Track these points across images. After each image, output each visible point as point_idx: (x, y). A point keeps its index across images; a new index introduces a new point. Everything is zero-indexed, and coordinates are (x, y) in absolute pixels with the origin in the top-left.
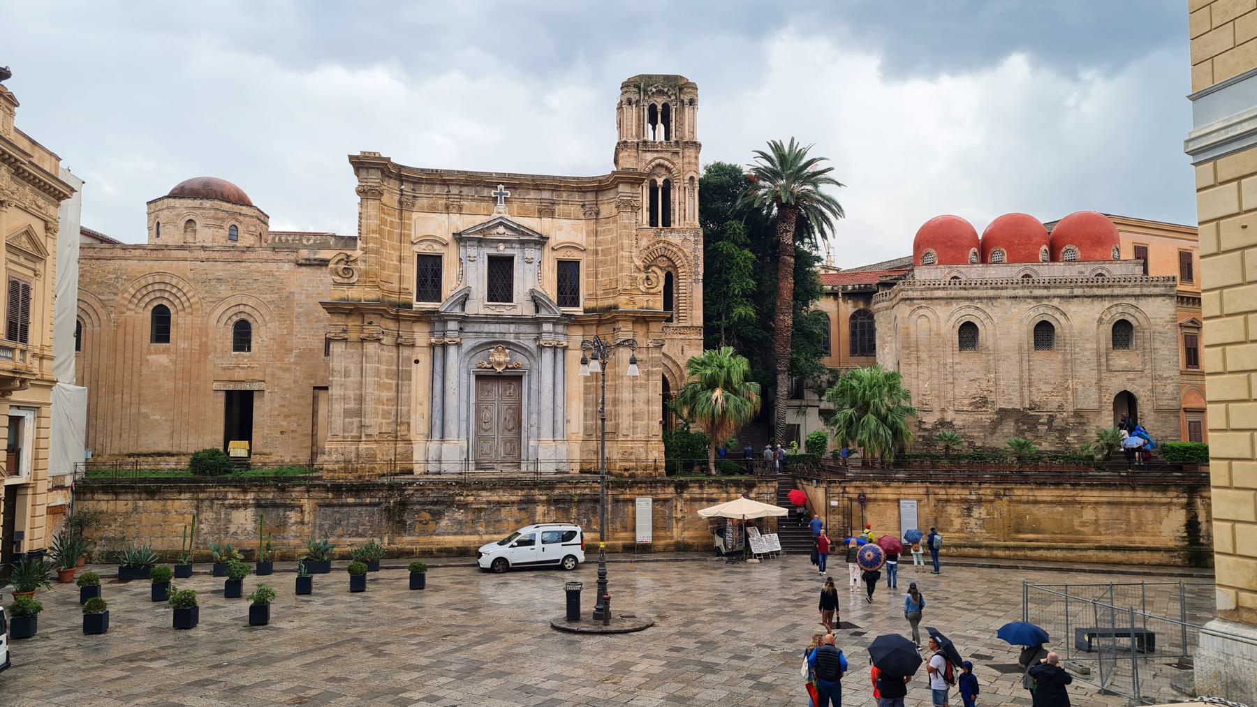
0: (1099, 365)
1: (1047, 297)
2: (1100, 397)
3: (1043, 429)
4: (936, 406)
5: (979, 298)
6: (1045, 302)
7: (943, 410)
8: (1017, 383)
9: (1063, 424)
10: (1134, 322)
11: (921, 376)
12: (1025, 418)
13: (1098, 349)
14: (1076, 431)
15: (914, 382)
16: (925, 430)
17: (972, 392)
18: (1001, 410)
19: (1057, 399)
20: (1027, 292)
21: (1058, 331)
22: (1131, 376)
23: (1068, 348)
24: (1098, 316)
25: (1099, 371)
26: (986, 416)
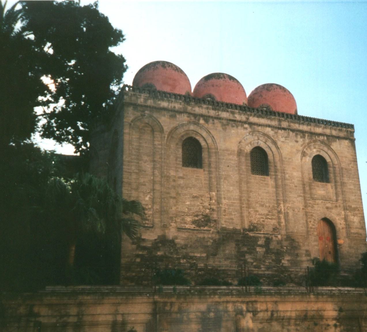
0: (304, 192)
1: (260, 125)
6: (260, 128)
9: (278, 247)
10: (328, 160)
12: (243, 239)
13: (303, 178)
14: (290, 254)
16: (145, 248)
17: (194, 209)
18: (224, 229)
19: (274, 222)
20: (243, 118)
21: (270, 157)
23: (279, 175)
24: (301, 148)
26: (209, 234)
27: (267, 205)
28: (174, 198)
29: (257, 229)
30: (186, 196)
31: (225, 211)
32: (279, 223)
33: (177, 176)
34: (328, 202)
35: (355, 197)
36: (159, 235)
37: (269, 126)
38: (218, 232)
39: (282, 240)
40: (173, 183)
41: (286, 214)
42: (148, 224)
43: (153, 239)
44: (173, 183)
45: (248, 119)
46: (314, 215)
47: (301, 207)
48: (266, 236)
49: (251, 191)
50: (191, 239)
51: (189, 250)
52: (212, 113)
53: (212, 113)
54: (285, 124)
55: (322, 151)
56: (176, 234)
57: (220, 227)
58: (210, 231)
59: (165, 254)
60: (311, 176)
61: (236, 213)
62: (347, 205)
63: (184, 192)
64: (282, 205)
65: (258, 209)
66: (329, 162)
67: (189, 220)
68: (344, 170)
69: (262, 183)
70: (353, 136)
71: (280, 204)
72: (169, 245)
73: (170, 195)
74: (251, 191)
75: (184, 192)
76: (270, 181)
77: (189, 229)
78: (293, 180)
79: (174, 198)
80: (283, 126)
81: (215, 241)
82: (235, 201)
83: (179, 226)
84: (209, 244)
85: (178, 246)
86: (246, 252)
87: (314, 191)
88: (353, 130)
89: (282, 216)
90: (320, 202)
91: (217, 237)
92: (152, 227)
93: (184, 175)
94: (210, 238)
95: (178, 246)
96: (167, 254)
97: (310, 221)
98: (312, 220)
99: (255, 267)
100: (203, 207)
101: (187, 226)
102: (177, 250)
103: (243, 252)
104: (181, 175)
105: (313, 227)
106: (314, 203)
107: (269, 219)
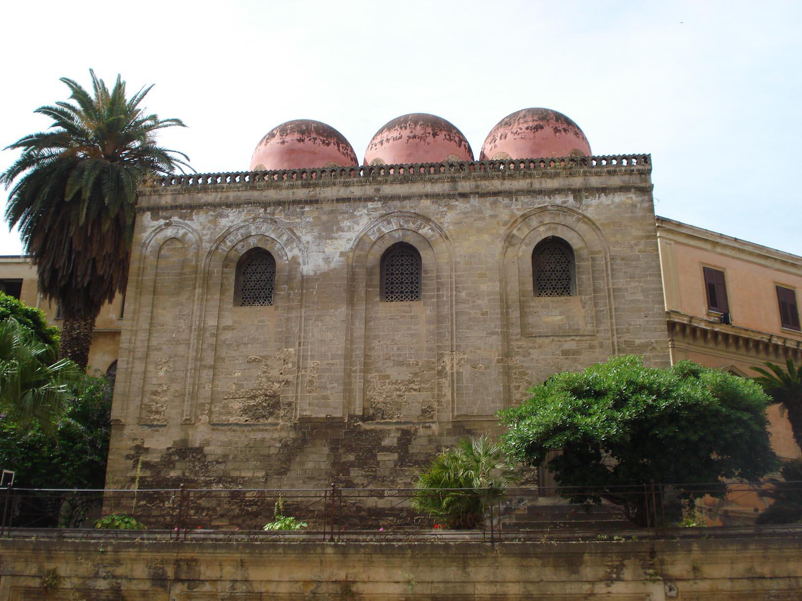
2: (508, 390)
3: (387, 459)
4: (174, 414)
5: (279, 203)
7: (188, 423)
8: (339, 365)
9: (431, 449)
11: (155, 356)
12: (349, 438)
15: (139, 367)
16: (146, 465)
17: (251, 384)
18: (304, 420)
20: (369, 190)
22: (570, 345)
23: (444, 292)
24: (503, 231)
25: (506, 337)
26: (276, 433)
27: (412, 361)
28: (210, 367)
29: (383, 414)
30: (236, 362)
31: (311, 382)
32: (439, 398)
33: (221, 327)
34: (568, 339)
35: (646, 319)
36: (177, 439)
37: (427, 196)
38: (295, 427)
39: (441, 434)
40: (212, 341)
41: (455, 375)
42: (158, 420)
43: (164, 447)
44: (212, 341)
45: (378, 190)
46: (529, 371)
47: (495, 357)
48: (404, 427)
49: (376, 337)
50: (236, 443)
51: (230, 466)
52: (302, 193)
53: (302, 193)
54: (465, 186)
55: (560, 227)
56: (207, 437)
57: (298, 417)
58: (277, 424)
59: (184, 473)
60: (530, 287)
61: (335, 385)
62: (622, 340)
63: (234, 354)
64: (446, 359)
65: (389, 372)
66: (580, 249)
67: (236, 407)
68: (618, 261)
69: (402, 317)
70: (648, 180)
71: (440, 356)
72: (193, 457)
73: (203, 363)
74: (376, 337)
75: (234, 354)
76: (420, 311)
77: (237, 424)
78: (479, 302)
79: (210, 367)
80: (460, 190)
81: (285, 446)
82: (335, 361)
83: (215, 420)
84: (273, 451)
85: (209, 458)
86: (352, 464)
87: (531, 320)
88: (647, 167)
89: (446, 382)
90: (547, 341)
91: (292, 435)
92: (165, 426)
93: (235, 322)
94: (275, 440)
95: (209, 458)
96: (187, 474)
97: (519, 387)
98: (523, 385)
99: (372, 494)
100: (268, 379)
101: (232, 419)
102: (207, 466)
103: (344, 463)
104: (230, 323)
105: (524, 399)
106: (531, 345)
107: (415, 390)
